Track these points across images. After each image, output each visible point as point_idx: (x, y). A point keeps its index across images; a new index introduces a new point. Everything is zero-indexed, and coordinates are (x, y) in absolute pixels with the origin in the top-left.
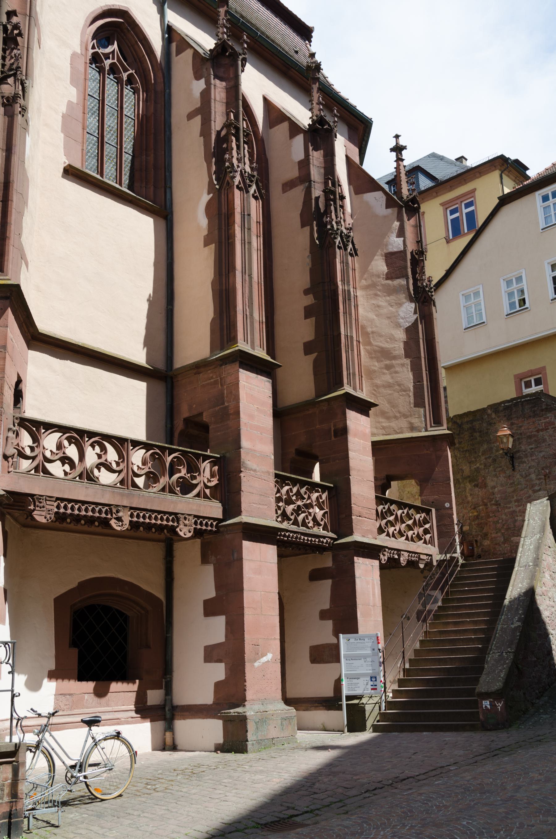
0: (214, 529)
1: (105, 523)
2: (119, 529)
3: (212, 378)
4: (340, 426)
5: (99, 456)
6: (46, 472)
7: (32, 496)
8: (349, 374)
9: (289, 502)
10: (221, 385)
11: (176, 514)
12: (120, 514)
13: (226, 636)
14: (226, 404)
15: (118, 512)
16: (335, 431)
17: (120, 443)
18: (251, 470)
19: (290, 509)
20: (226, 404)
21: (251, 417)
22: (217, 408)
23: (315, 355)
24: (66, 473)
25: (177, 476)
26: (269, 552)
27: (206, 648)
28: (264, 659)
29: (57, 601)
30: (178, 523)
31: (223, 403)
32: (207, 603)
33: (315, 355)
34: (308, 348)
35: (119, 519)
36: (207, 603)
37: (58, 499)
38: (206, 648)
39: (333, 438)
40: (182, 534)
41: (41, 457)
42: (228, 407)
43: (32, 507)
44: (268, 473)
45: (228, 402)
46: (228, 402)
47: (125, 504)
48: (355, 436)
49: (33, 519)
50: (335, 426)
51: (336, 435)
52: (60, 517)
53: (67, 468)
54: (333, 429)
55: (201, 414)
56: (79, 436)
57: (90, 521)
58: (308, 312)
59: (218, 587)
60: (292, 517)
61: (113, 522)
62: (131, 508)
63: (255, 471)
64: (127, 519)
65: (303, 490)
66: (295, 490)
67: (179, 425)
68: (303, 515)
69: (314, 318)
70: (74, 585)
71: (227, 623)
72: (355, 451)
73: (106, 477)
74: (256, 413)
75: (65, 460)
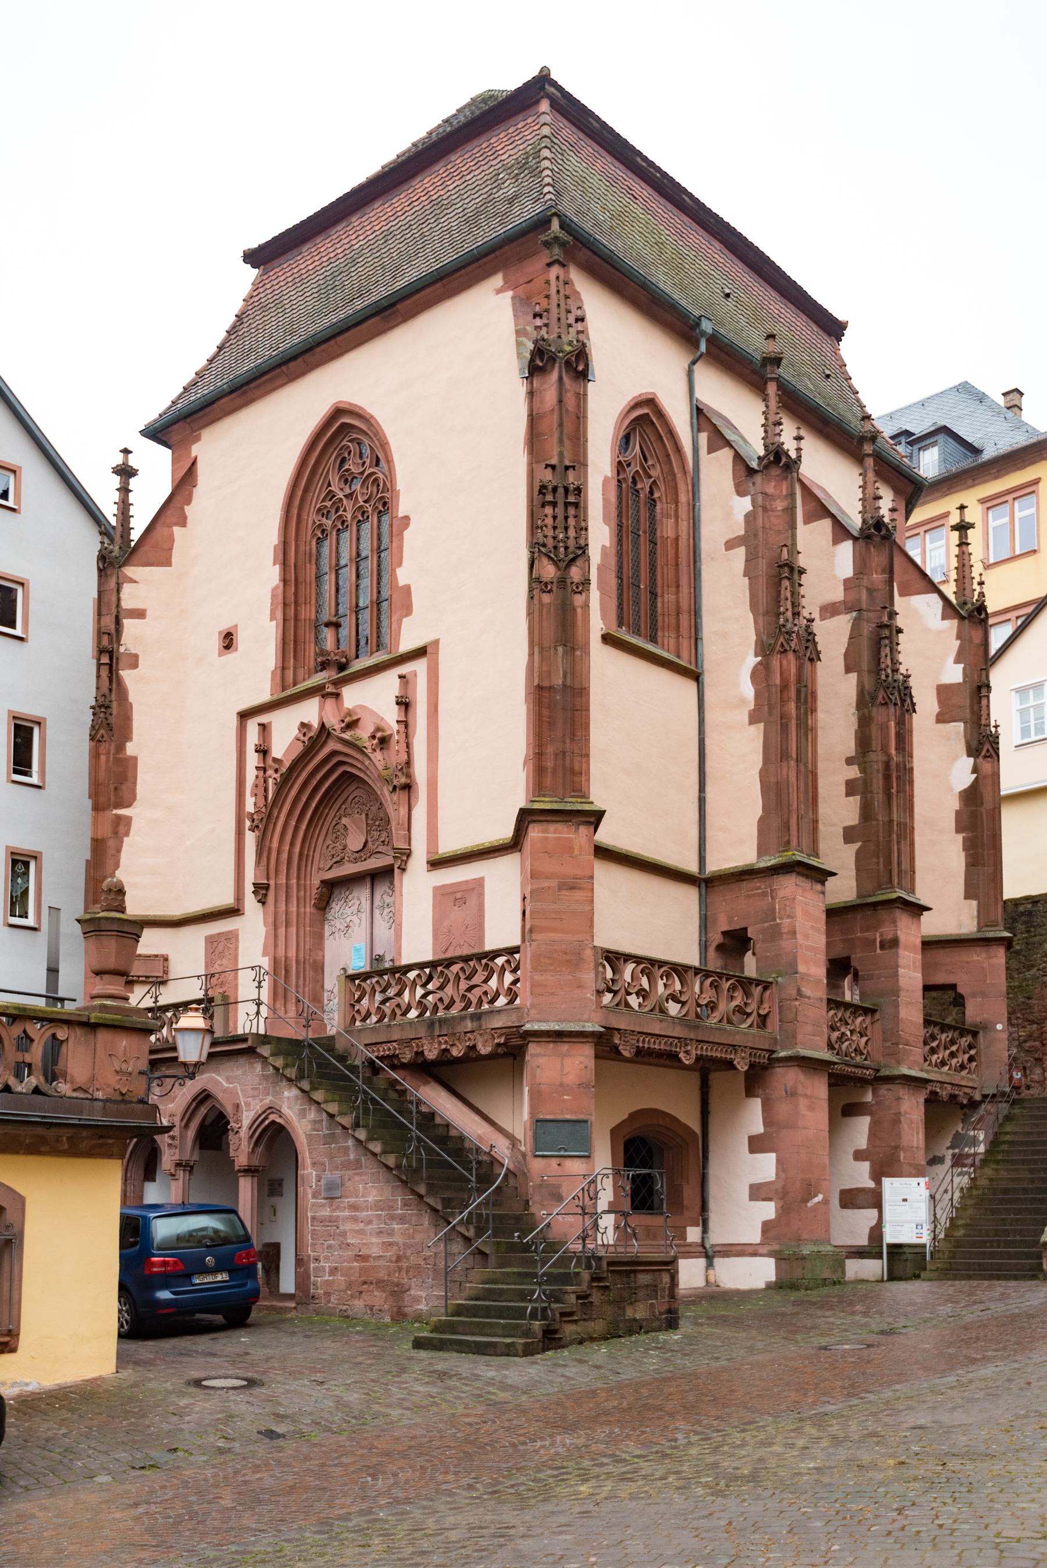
0: (766, 1061)
1: (674, 1057)
2: (687, 1062)
3: (759, 888)
4: (890, 936)
5: (665, 985)
6: (627, 1005)
7: (619, 1030)
8: (900, 872)
9: (833, 1028)
10: (772, 898)
11: (734, 1046)
12: (689, 1048)
13: (777, 1174)
14: (778, 921)
15: (686, 1045)
16: (881, 942)
17: (679, 970)
18: (805, 997)
19: (836, 1035)
20: (778, 921)
21: (806, 937)
22: (766, 925)
23: (859, 844)
24: (640, 1005)
25: (734, 1004)
26: (819, 1088)
27: (752, 1187)
28: (816, 1200)
29: (614, 1132)
30: (735, 1054)
31: (775, 920)
32: (752, 1140)
33: (859, 844)
34: (849, 835)
35: (686, 1052)
36: (752, 1140)
37: (639, 1033)
38: (752, 1187)
39: (878, 951)
40: (739, 1067)
41: (623, 991)
42: (778, 925)
43: (617, 1041)
44: (821, 999)
45: (781, 919)
46: (781, 919)
47: (692, 1036)
48: (906, 948)
49: (620, 1053)
50: (881, 935)
51: (882, 947)
52: (639, 1052)
53: (641, 1000)
54: (878, 940)
55: (746, 929)
56: (649, 965)
57: (660, 1054)
58: (851, 788)
59: (766, 1124)
60: (837, 1046)
61: (681, 1055)
62: (697, 1041)
63: (809, 998)
64: (694, 1052)
65: (848, 1013)
66: (840, 1015)
67: (716, 938)
68: (847, 1043)
69: (859, 797)
70: (626, 1116)
71: (778, 1161)
72: (904, 968)
73: (673, 1009)
74: (811, 932)
75: (642, 993)
